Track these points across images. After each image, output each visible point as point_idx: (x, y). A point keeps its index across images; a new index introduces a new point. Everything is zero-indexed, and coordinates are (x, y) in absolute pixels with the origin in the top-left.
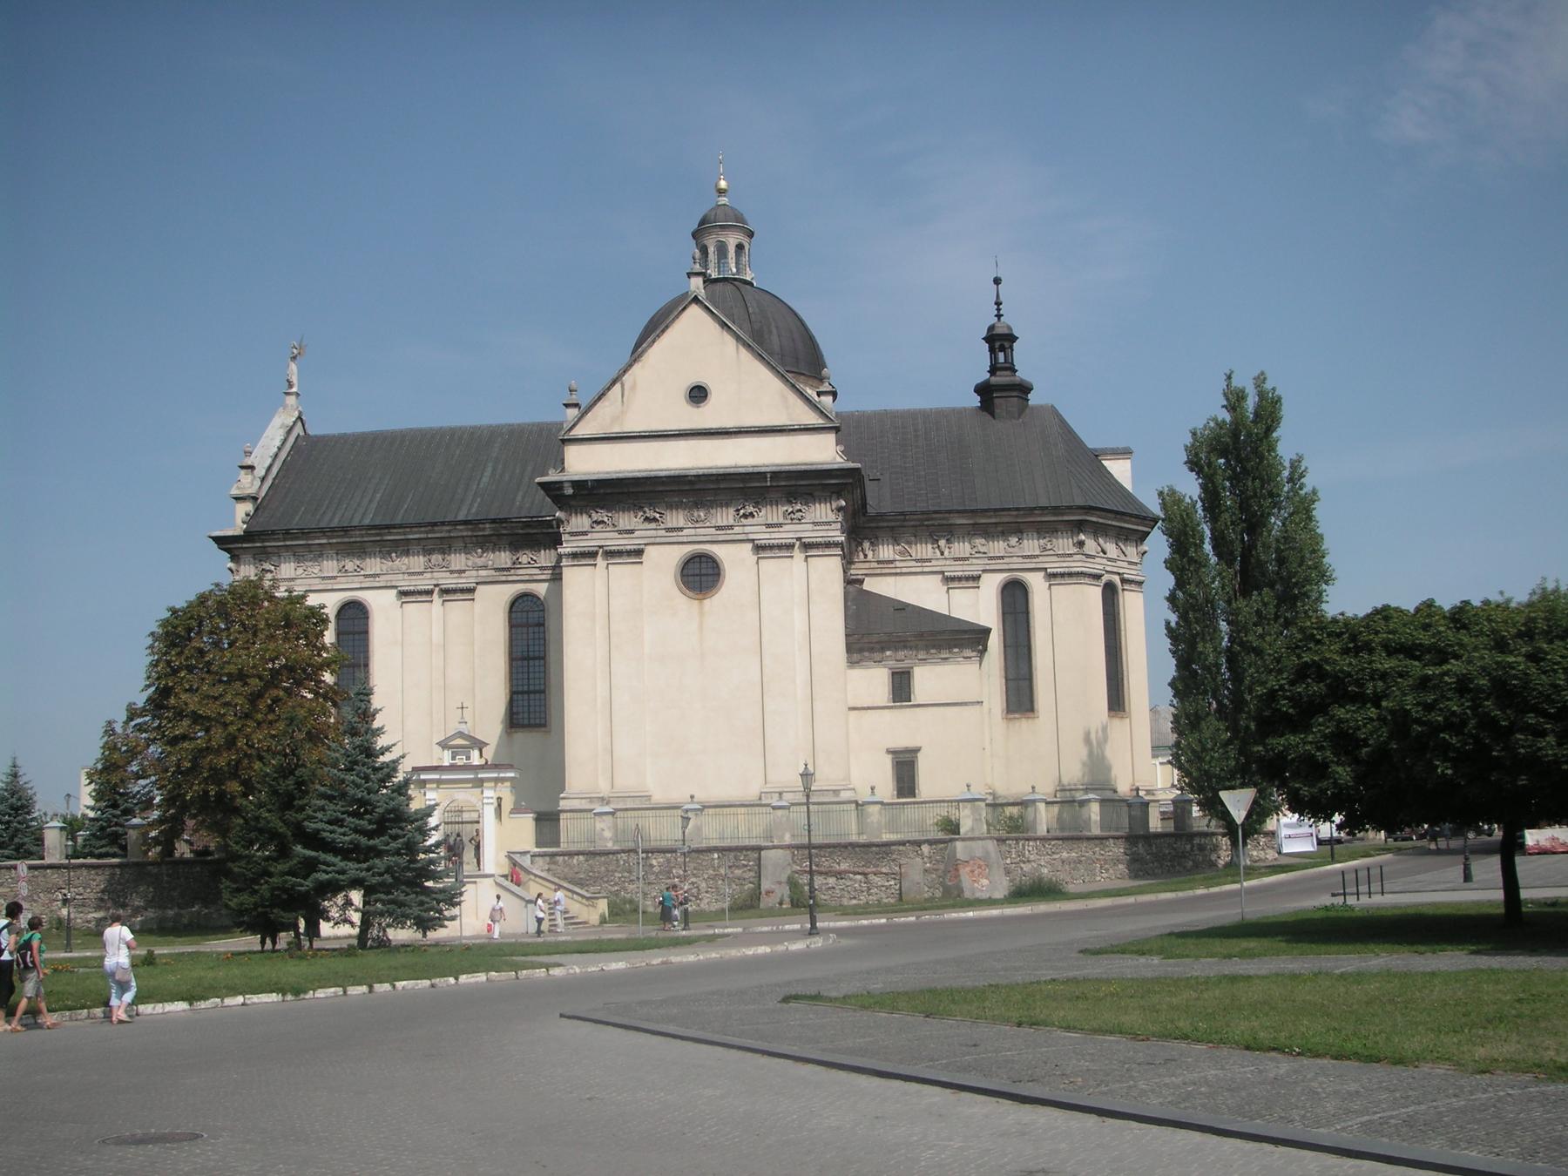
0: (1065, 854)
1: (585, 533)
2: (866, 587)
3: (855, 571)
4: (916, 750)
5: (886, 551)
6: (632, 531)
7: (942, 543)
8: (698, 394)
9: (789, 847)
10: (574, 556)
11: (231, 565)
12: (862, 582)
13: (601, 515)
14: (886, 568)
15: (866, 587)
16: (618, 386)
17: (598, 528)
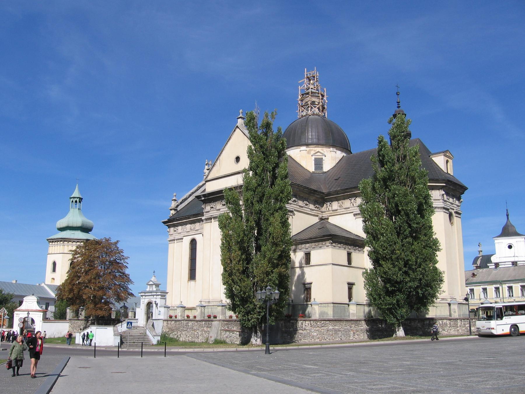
0: (331, 327)
1: (209, 212)
2: (329, 221)
3: (325, 215)
4: (311, 284)
5: (335, 205)
6: (219, 210)
7: (353, 201)
8: (238, 159)
9: (219, 320)
10: (206, 219)
11: (168, 230)
12: (328, 219)
13: (212, 205)
14: (335, 213)
15: (329, 221)
16: (218, 161)
17: (212, 209)
